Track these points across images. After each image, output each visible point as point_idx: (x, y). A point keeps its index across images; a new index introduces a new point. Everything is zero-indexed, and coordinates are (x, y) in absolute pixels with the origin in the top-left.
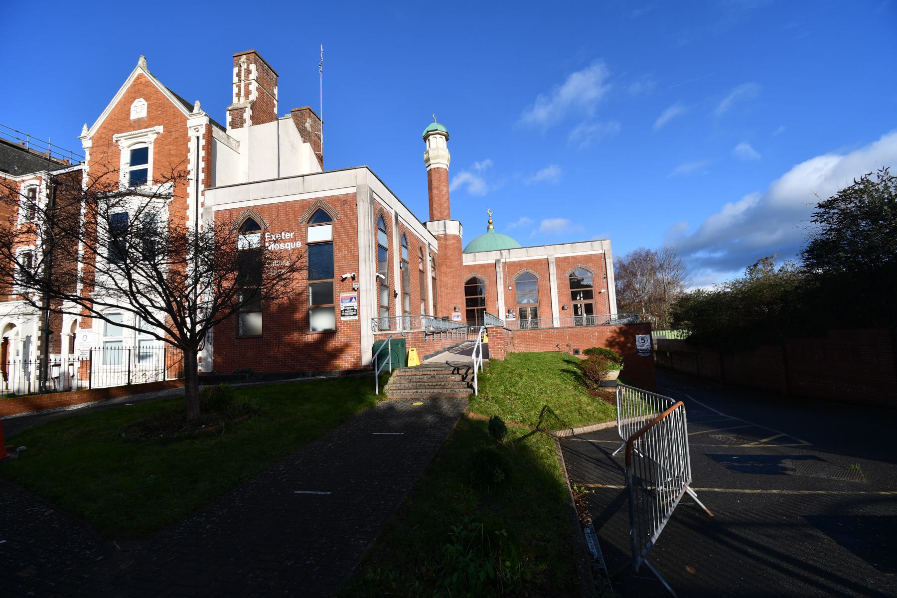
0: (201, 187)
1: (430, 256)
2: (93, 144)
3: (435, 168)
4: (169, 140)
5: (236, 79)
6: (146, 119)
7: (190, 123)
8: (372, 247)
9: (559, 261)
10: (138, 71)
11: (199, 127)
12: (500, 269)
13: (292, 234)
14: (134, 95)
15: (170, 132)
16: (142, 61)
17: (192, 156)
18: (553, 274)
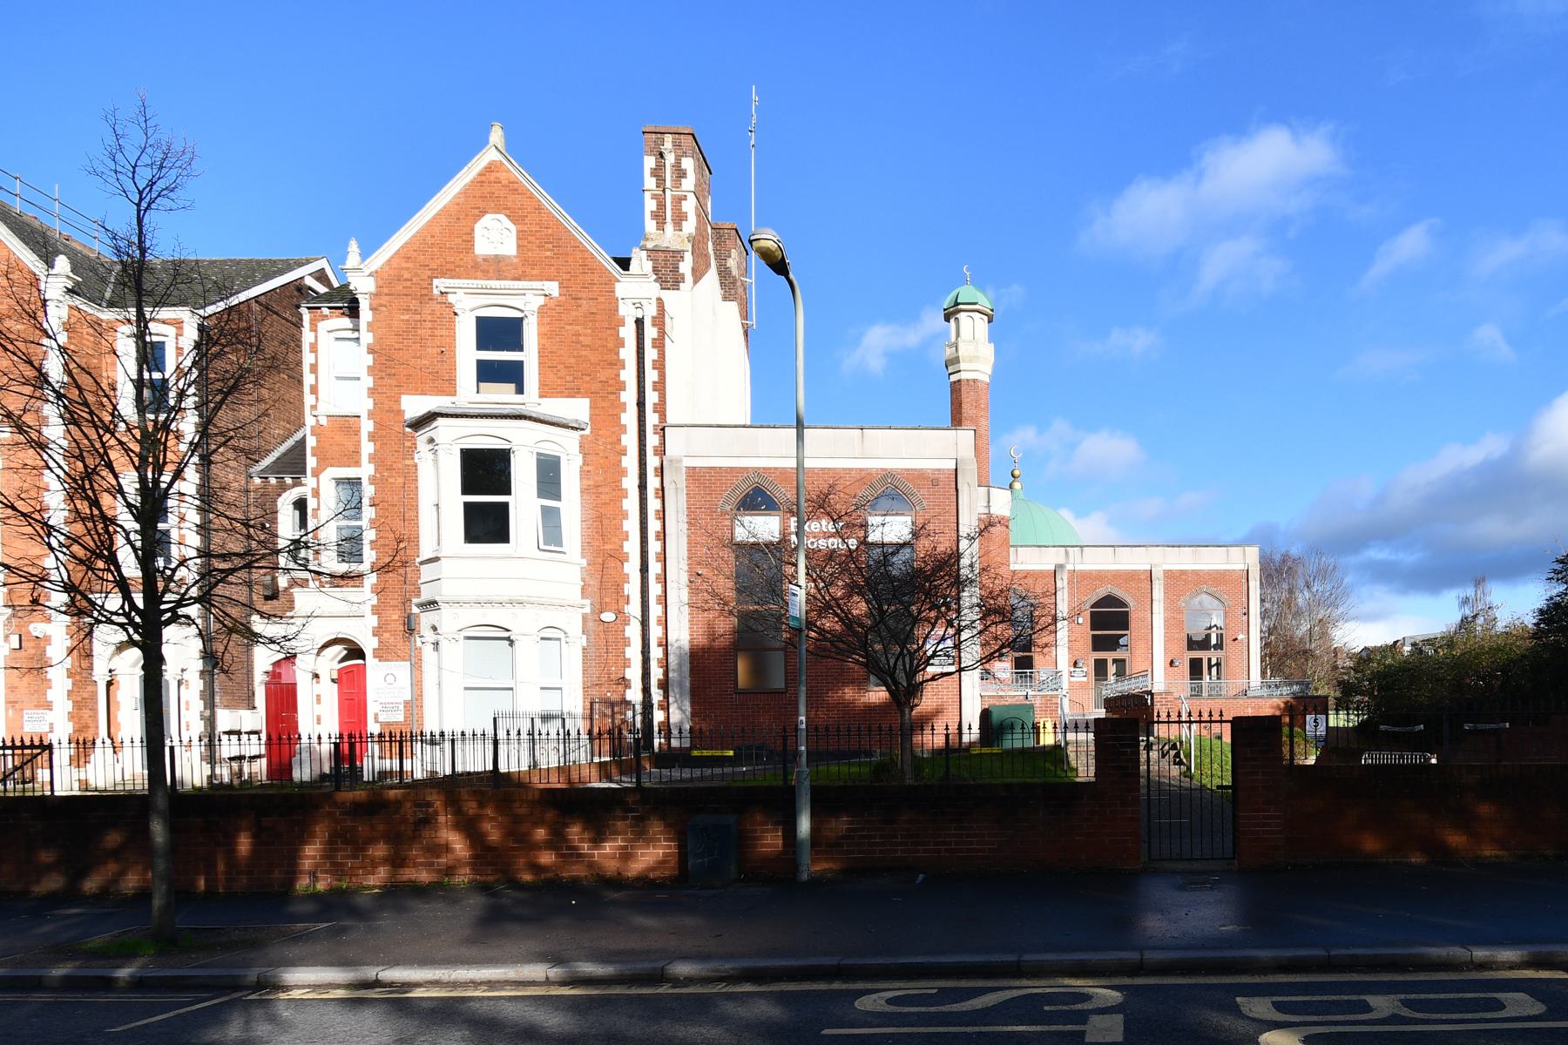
2: (378, 287)
3: (968, 380)
4: (574, 313)
5: (650, 182)
6: (515, 261)
9: (1170, 576)
10: (489, 155)
11: (643, 302)
14: (481, 204)
16: (496, 135)
18: (1159, 601)
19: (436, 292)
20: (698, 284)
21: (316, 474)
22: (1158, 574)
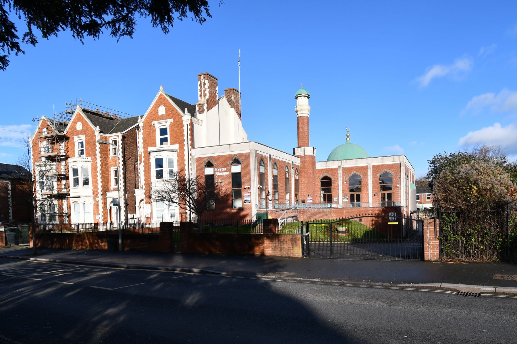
0: (190, 147)
2: (144, 125)
3: (300, 117)
4: (175, 125)
5: (199, 88)
6: (165, 115)
7: (184, 118)
8: (256, 175)
9: (374, 167)
10: (161, 92)
12: (340, 172)
13: (226, 169)
14: (159, 104)
16: (161, 88)
17: (185, 133)
18: (370, 175)
19: (153, 124)
20: (209, 111)
21: (140, 165)
22: (370, 167)
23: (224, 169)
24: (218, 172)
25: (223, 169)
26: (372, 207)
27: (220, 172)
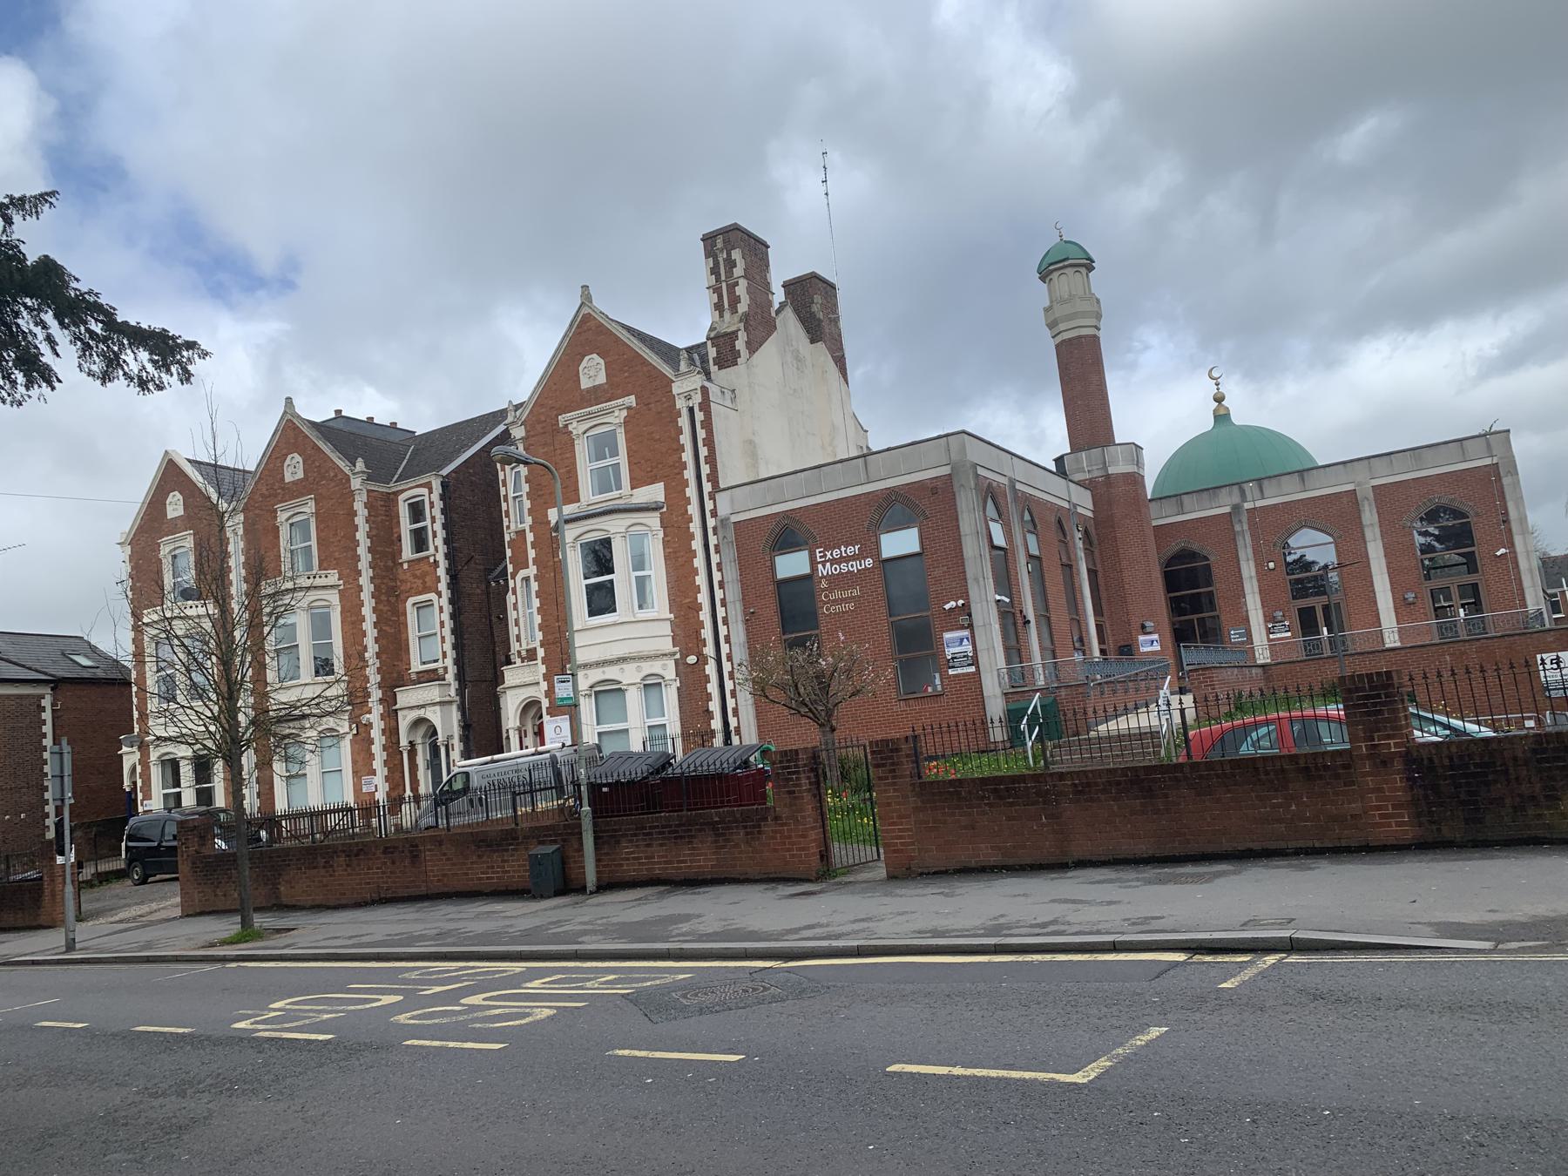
1: (1079, 531)
2: (527, 432)
7: (676, 389)
8: (985, 556)
11: (692, 393)
12: (1242, 527)
13: (857, 547)
15: (648, 404)
23: (851, 550)
24: (828, 565)
25: (848, 551)
26: (1398, 644)
27: (833, 561)
